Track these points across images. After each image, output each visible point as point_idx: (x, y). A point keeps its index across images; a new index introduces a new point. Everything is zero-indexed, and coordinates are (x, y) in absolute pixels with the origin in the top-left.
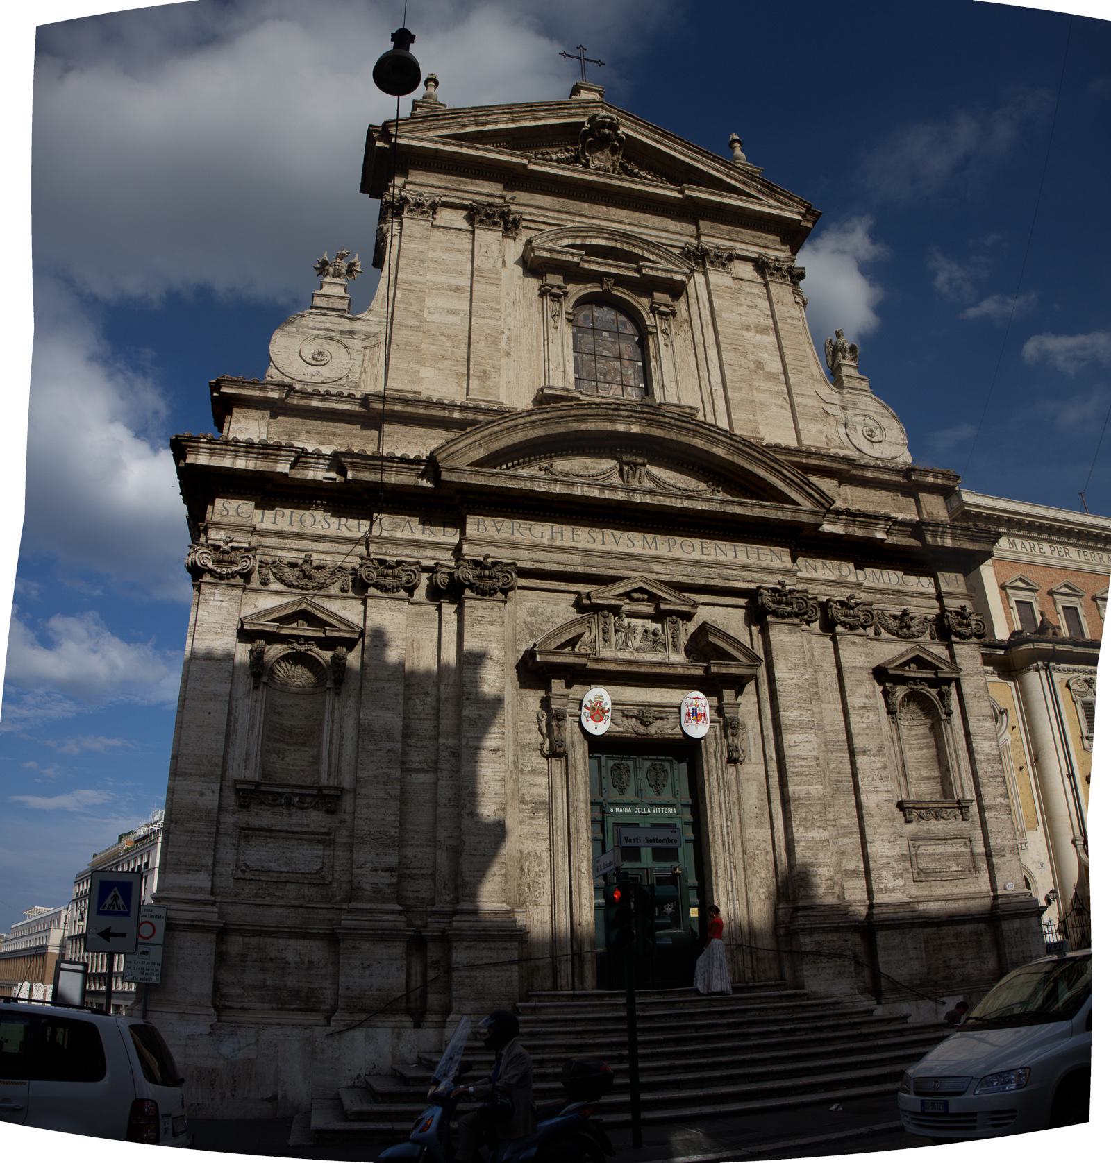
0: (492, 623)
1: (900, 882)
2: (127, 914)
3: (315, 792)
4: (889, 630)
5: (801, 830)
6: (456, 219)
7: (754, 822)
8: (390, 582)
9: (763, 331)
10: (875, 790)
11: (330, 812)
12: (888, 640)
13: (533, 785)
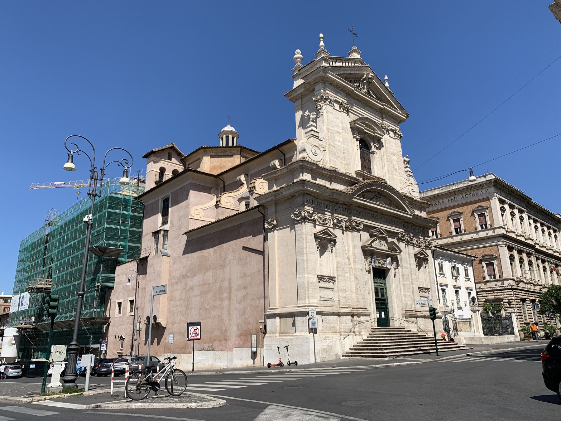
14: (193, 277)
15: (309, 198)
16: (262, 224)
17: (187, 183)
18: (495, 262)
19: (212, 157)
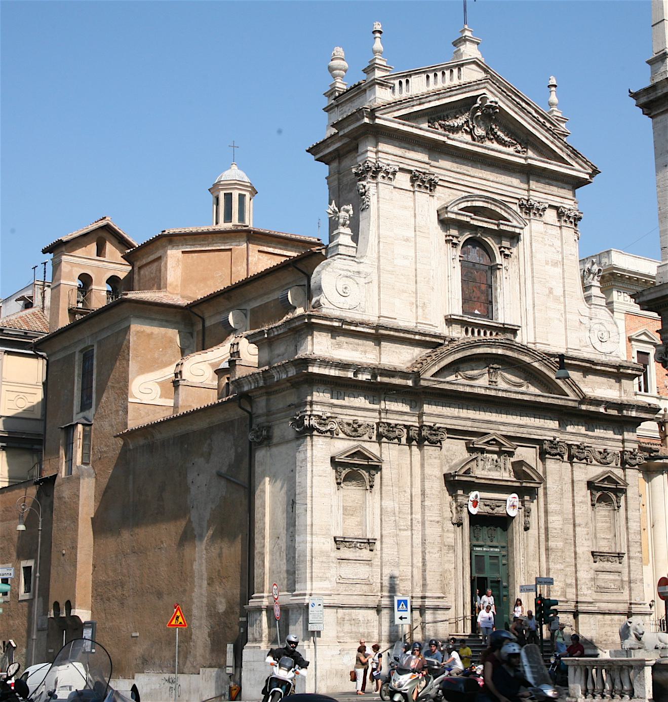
0: (435, 458)
1: (590, 592)
2: (407, 611)
3: (366, 541)
4: (596, 460)
5: (553, 564)
6: (403, 180)
7: (532, 559)
8: (392, 435)
9: (555, 264)
10: (583, 546)
11: (371, 550)
12: (595, 465)
13: (448, 537)
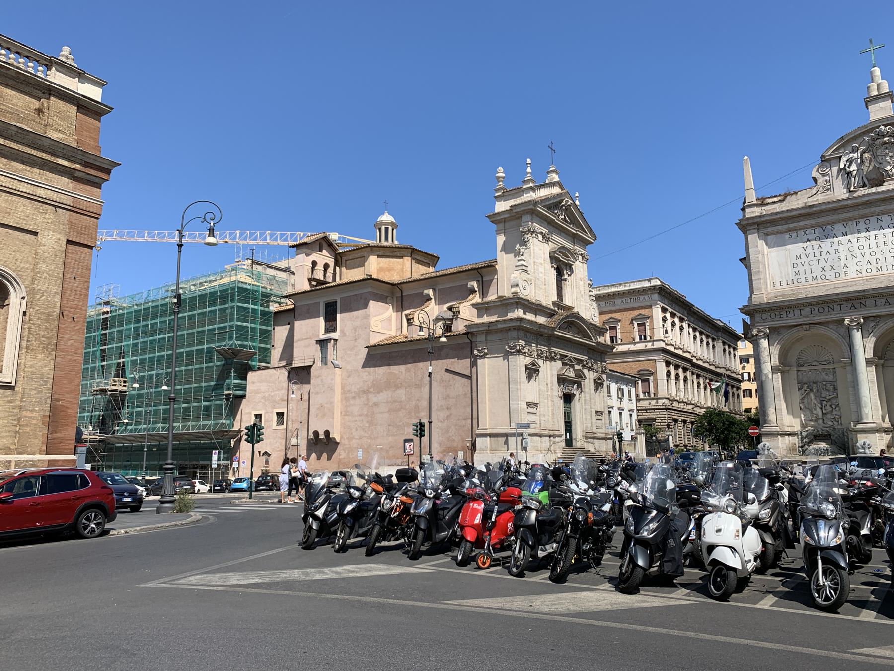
6: (540, 237)
14: (379, 393)
15: (522, 333)
16: (469, 349)
17: (366, 291)
18: (651, 378)
19: (379, 256)
